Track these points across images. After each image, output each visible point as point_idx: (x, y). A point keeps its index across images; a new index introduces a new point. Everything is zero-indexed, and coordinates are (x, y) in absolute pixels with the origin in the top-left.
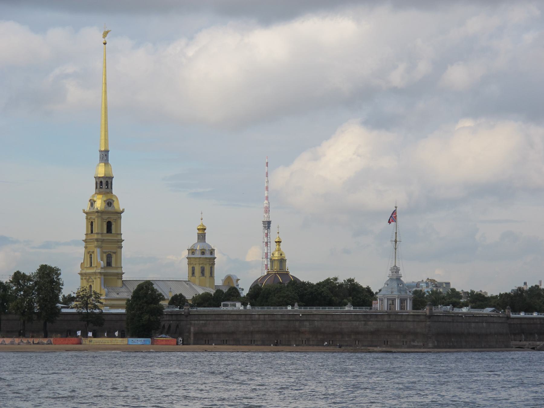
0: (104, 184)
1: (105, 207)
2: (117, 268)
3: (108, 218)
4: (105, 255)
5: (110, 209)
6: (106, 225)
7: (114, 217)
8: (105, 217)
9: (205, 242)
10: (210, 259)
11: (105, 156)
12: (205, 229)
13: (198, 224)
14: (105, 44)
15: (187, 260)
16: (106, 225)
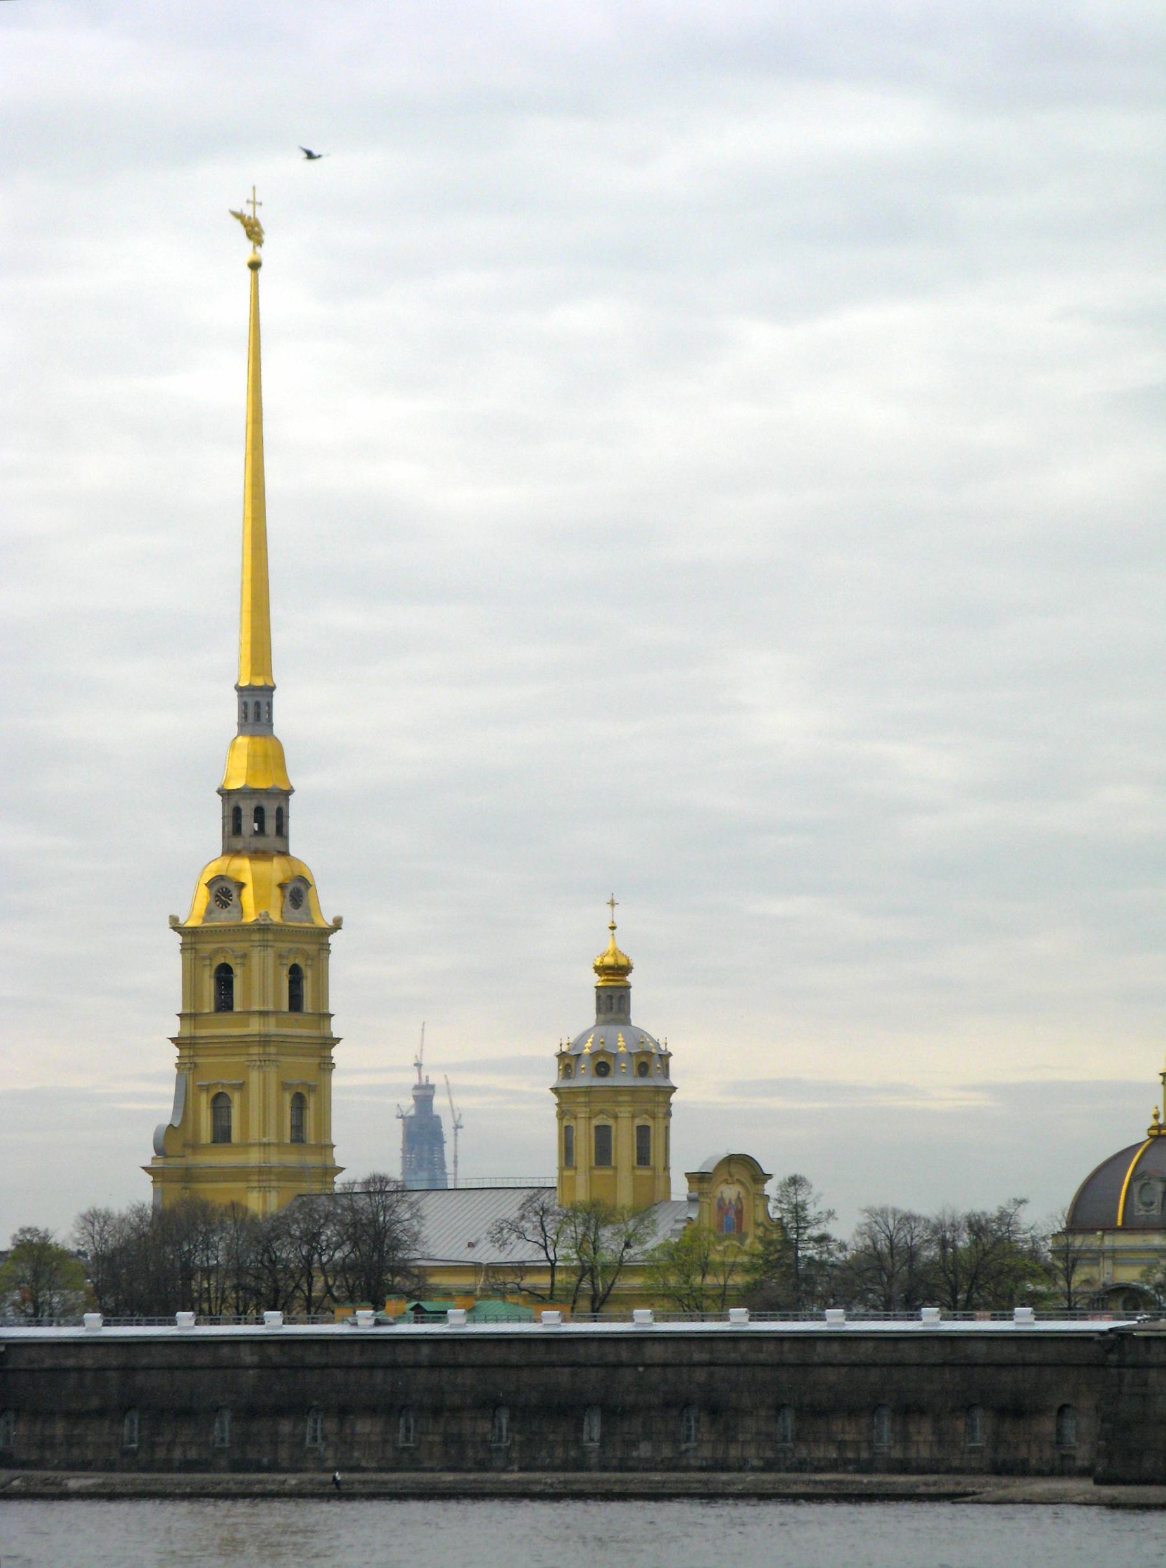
0: (256, 818)
1: (209, 912)
2: (246, 1146)
3: (216, 952)
4: (204, 1100)
5: (223, 918)
6: (257, 978)
7: (240, 947)
8: (207, 948)
9: (626, 1021)
10: (589, 1091)
11: (256, 708)
12: (625, 970)
13: (601, 949)
14: (255, 266)
15: (555, 1099)
16: (257, 978)
